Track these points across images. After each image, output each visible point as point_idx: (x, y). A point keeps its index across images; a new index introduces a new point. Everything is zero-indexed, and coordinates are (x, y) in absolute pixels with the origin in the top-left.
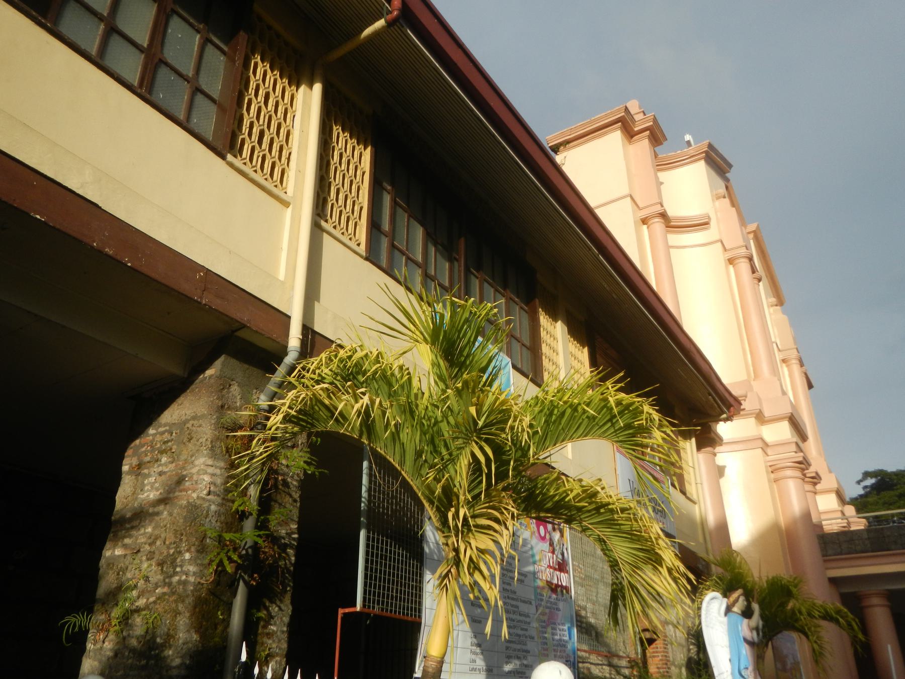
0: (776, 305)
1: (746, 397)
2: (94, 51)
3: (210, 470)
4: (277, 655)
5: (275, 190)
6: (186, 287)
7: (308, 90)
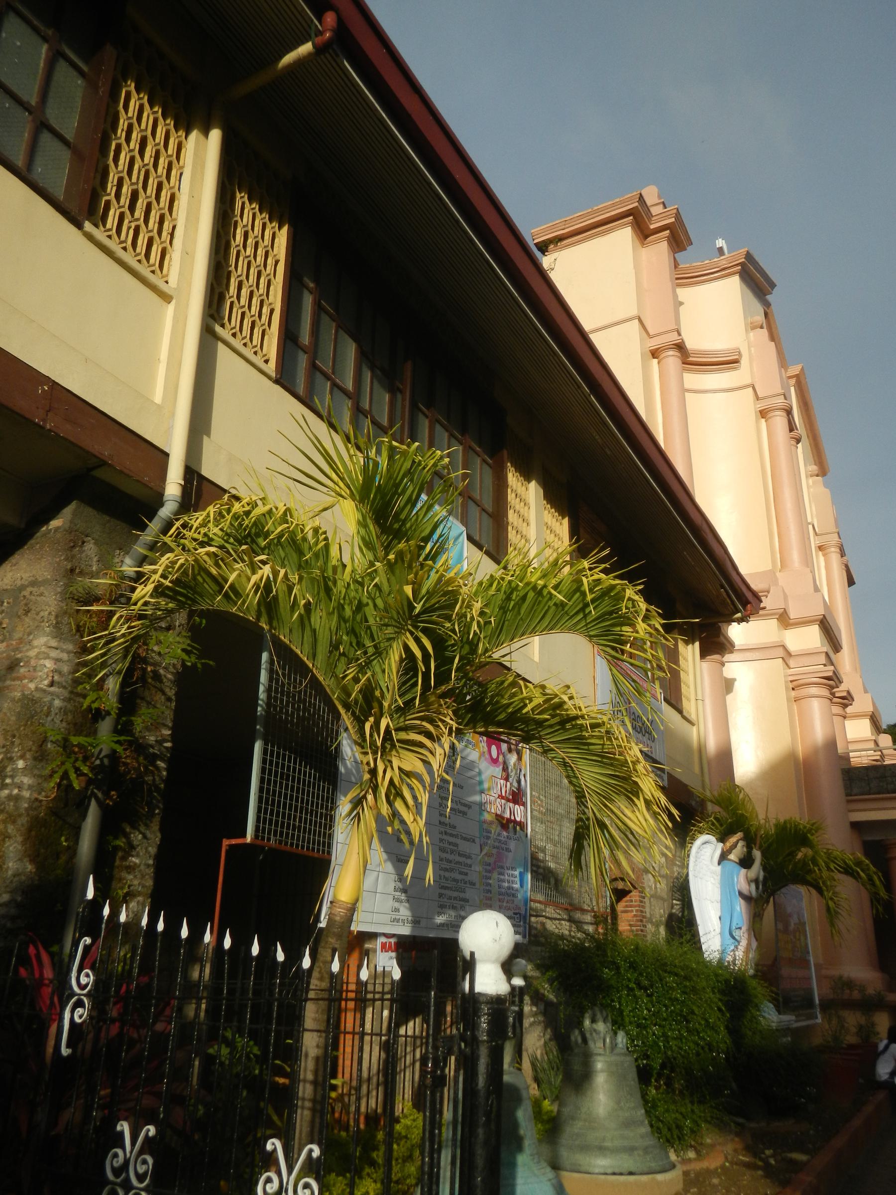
0: (817, 476)
1: (768, 592)
3: (54, 654)
4: (140, 894)
5: (152, 278)
6: (22, 404)
7: (202, 137)
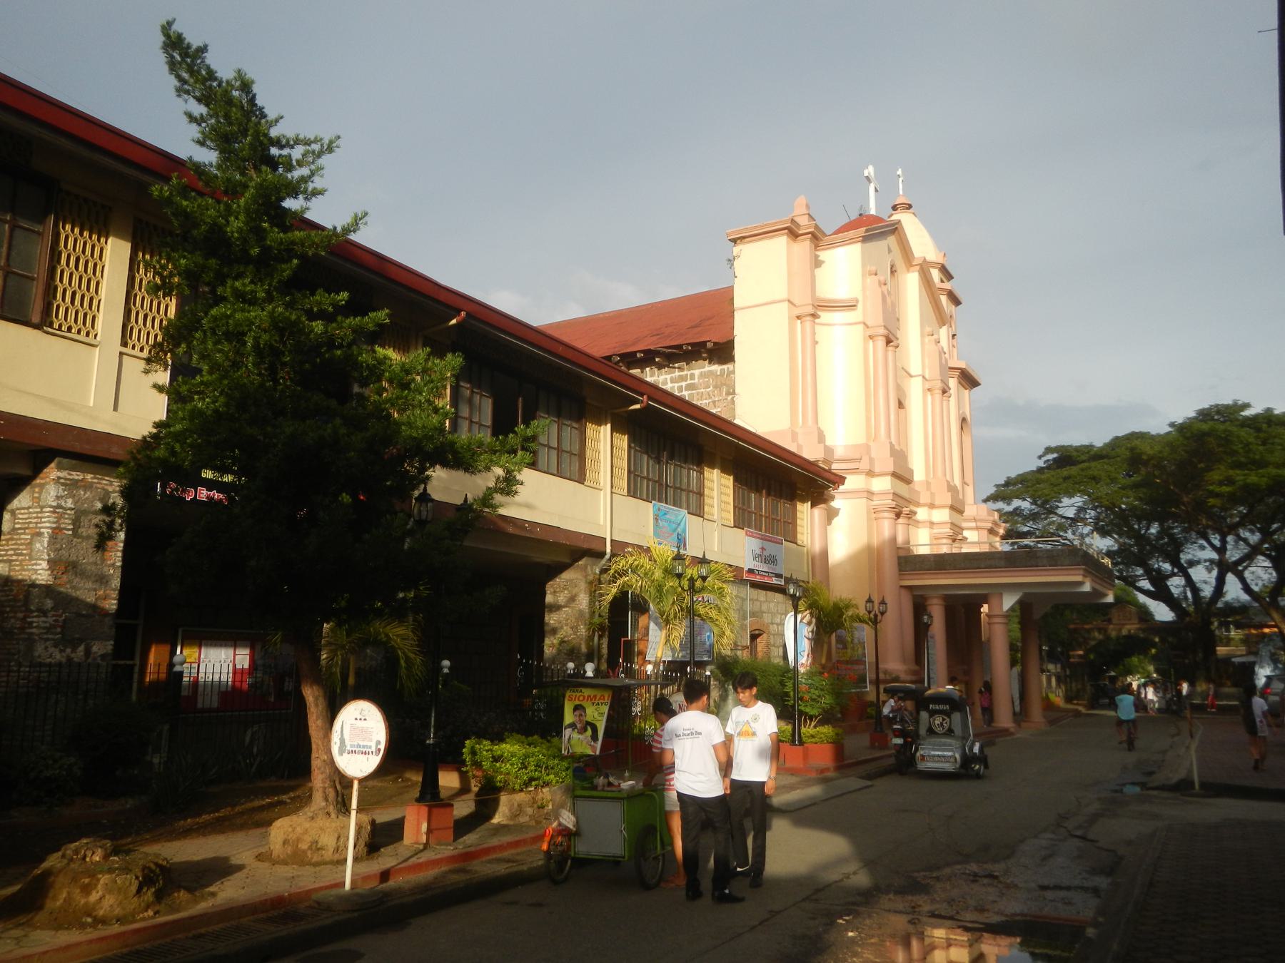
1: (861, 459)
2: (556, 472)
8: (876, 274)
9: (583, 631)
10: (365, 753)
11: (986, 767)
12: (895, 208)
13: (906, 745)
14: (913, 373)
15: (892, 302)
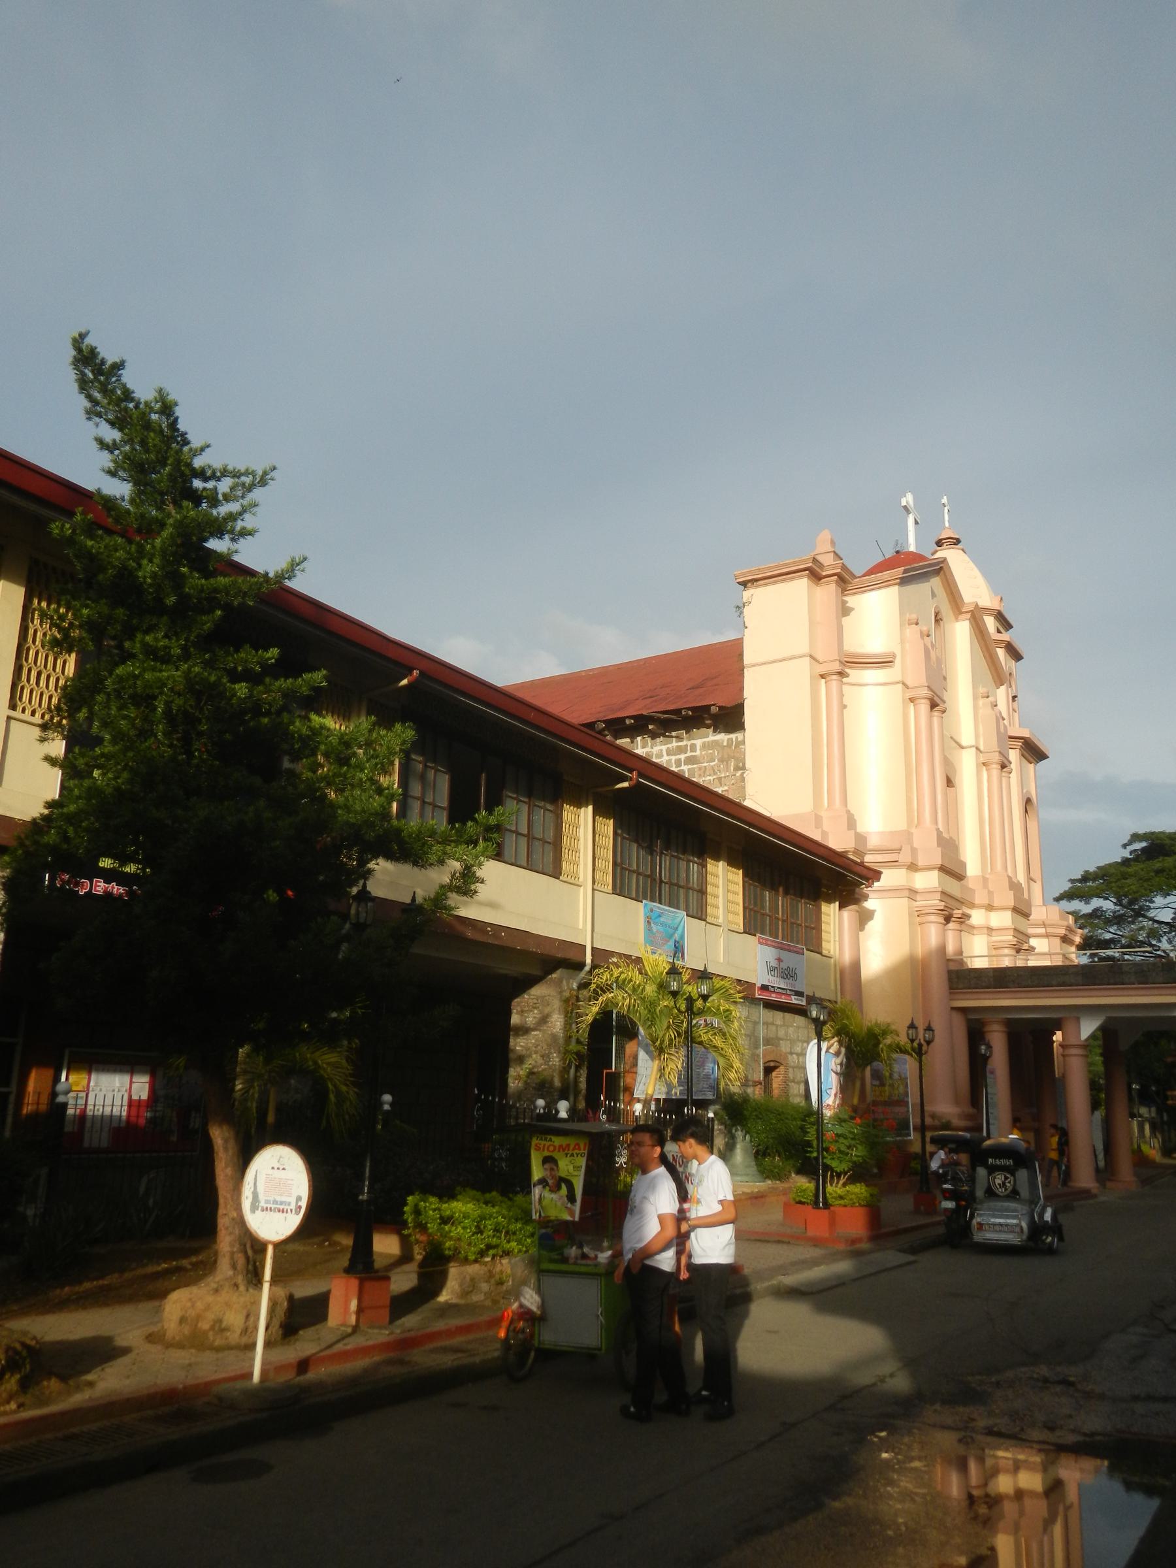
8: (917, 624)
9: (556, 1060)
10: (283, 1212)
11: (1061, 1239)
12: (939, 543)
13: (959, 1211)
14: (964, 744)
15: (937, 658)
